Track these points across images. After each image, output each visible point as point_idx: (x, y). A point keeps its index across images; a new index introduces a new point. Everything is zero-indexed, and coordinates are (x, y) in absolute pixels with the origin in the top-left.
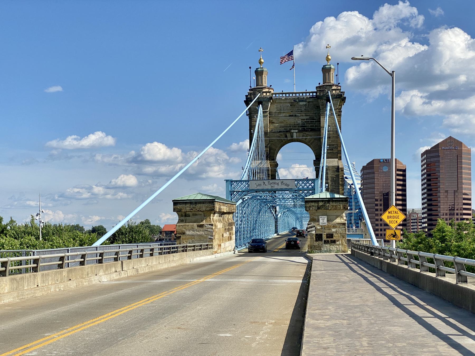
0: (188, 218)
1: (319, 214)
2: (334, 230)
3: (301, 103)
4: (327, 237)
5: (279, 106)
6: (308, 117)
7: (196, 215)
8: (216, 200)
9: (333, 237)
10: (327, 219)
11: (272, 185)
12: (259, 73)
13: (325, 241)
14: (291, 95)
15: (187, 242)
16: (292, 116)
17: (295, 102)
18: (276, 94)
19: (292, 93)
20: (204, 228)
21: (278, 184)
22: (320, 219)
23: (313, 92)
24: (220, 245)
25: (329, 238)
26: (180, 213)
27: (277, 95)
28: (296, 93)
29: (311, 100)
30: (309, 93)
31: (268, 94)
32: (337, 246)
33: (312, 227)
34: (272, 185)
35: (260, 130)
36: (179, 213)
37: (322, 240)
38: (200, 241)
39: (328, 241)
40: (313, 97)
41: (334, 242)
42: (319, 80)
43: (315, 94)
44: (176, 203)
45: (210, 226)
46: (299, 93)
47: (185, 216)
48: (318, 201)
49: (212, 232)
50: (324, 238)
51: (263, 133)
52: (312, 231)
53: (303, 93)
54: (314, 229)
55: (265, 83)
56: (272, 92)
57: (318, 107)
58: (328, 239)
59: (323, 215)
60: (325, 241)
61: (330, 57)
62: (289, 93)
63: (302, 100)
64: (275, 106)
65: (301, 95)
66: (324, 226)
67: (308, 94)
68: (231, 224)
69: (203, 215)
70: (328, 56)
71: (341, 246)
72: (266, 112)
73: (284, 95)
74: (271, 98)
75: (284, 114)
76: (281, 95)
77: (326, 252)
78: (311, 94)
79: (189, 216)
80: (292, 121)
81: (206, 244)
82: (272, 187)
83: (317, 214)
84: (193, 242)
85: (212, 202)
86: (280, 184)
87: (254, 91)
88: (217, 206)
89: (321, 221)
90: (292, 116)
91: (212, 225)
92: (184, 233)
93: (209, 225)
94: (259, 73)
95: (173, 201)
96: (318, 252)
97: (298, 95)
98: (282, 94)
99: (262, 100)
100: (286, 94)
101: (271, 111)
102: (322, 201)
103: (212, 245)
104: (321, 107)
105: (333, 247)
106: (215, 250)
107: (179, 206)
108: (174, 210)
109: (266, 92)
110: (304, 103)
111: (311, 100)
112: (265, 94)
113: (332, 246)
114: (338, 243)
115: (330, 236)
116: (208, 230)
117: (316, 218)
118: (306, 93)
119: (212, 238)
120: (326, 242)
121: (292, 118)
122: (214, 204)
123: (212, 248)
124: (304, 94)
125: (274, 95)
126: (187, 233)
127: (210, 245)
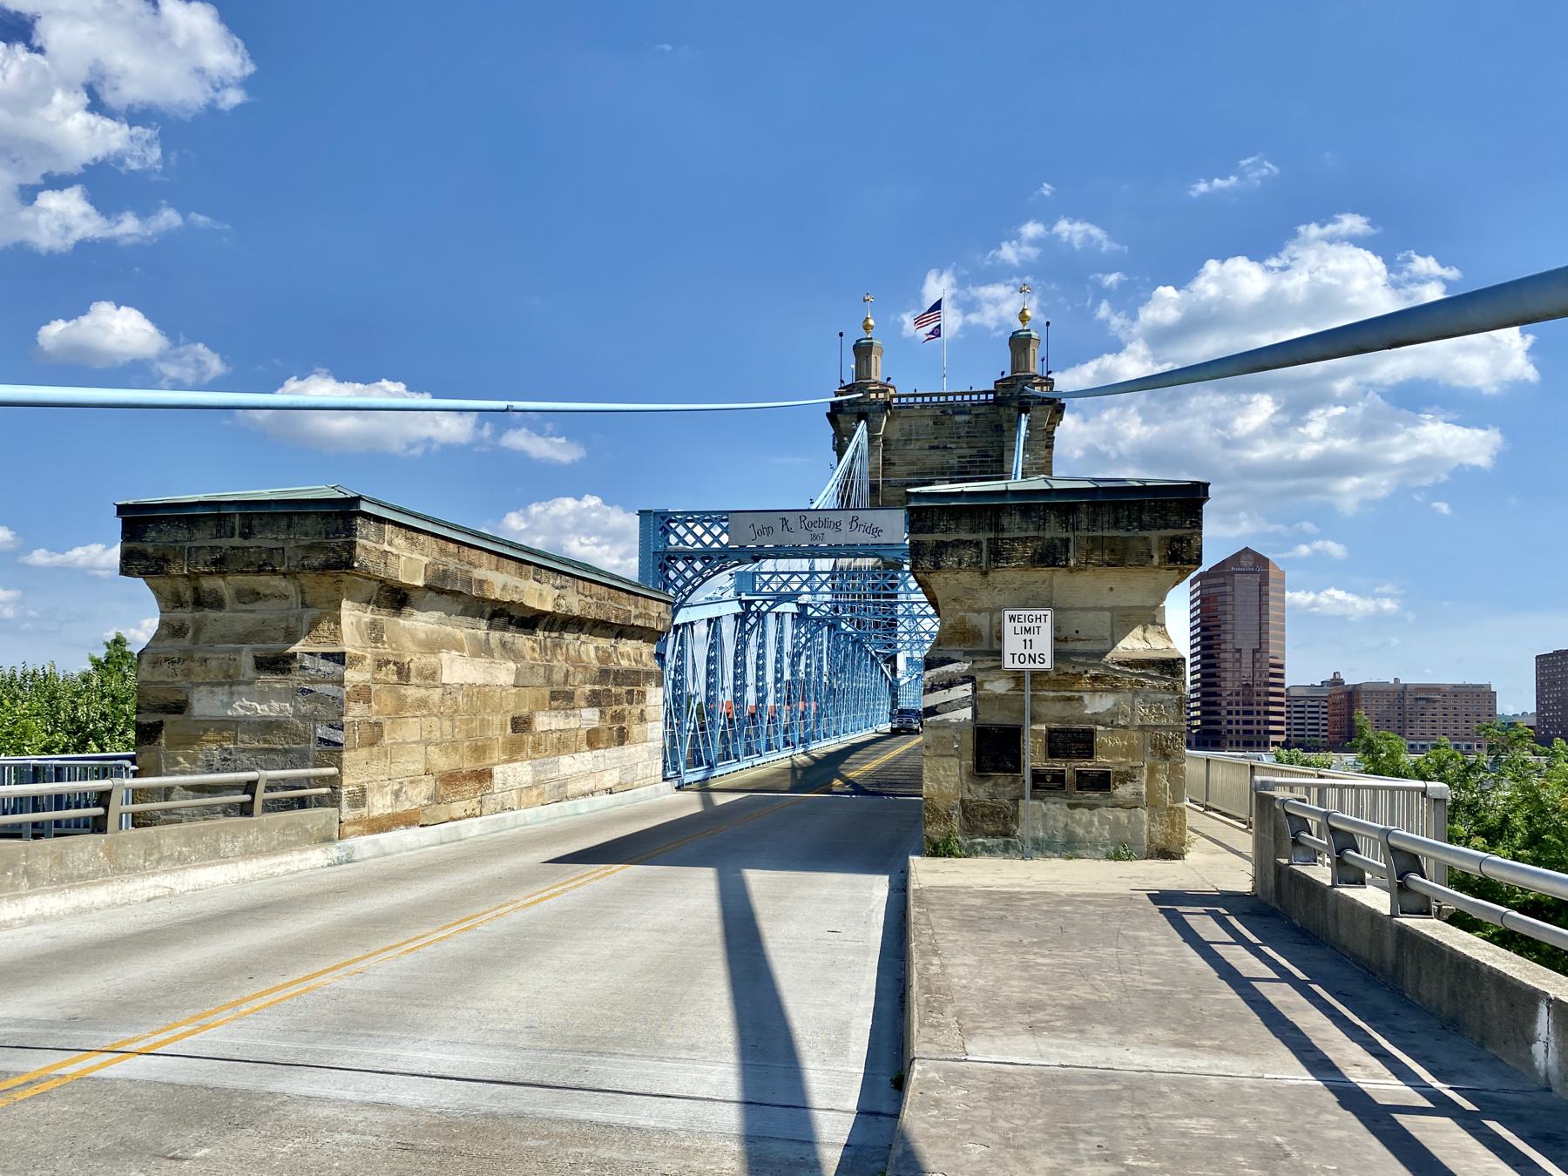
0: (212, 614)
1: (1000, 600)
2: (1098, 704)
3: (959, 418)
4: (1052, 753)
5: (906, 426)
6: (974, 452)
7: (256, 596)
8: (365, 507)
9: (1089, 753)
10: (1057, 628)
11: (815, 531)
12: (863, 351)
13: (1038, 777)
14: (935, 399)
15: (193, 760)
16: (936, 448)
17: (945, 411)
18: (900, 397)
19: (939, 395)
20: (296, 679)
21: (837, 526)
22: (1008, 627)
23: (987, 393)
24: (483, 776)
25: (1068, 756)
26: (166, 584)
27: (903, 400)
28: (947, 395)
29: (983, 410)
30: (978, 393)
31: (881, 395)
32: (1122, 815)
33: (950, 685)
34: (815, 531)
35: (857, 466)
36: (159, 582)
37: (1017, 768)
38: (269, 757)
39: (1059, 778)
40: (986, 403)
41: (1101, 782)
42: (1000, 365)
43: (991, 397)
44: (138, 522)
45: (328, 667)
46: (954, 394)
47: (199, 602)
48: (998, 510)
49: (338, 704)
50: (1033, 755)
51: (866, 488)
52: (950, 706)
53: (963, 394)
54: (963, 691)
55: (878, 374)
56: (892, 391)
57: (999, 429)
58: (1059, 765)
59: (1025, 605)
60: (1038, 777)
61: (1028, 313)
62: (931, 395)
63: (959, 410)
64: (897, 424)
65: (959, 398)
66: (1035, 675)
67: (975, 397)
68: (633, 679)
69: (295, 599)
70: (1023, 311)
71: (1144, 814)
72: (877, 438)
73: (919, 400)
74: (888, 405)
75: (918, 444)
76: (911, 400)
77: (1043, 848)
78: (983, 397)
79: (218, 604)
80: (936, 459)
81: (297, 776)
82: (815, 537)
83: (985, 599)
84: (227, 764)
85: (342, 515)
86: (845, 527)
87: (850, 389)
88: (367, 542)
89: (1012, 644)
90: (936, 448)
91: (339, 658)
92: (180, 708)
93: (326, 656)
94: (863, 351)
95: (121, 509)
96: (990, 851)
97: (951, 398)
98: (915, 396)
99: (866, 407)
100: (923, 395)
101: (889, 436)
102: (1026, 511)
103: (334, 782)
104: (1005, 426)
105: (1093, 821)
106: (380, 804)
107: (153, 542)
108: (130, 563)
109: (877, 392)
110: (966, 418)
111: (983, 410)
112: (873, 396)
113: (1082, 814)
114: (1123, 791)
115: (1073, 741)
116: (318, 688)
117: (982, 621)
118: (971, 394)
119: (338, 737)
120: (1044, 783)
121: (937, 452)
122: (351, 531)
123: (333, 800)
124: (967, 398)
125: (895, 400)
126: (205, 704)
127: (322, 781)
